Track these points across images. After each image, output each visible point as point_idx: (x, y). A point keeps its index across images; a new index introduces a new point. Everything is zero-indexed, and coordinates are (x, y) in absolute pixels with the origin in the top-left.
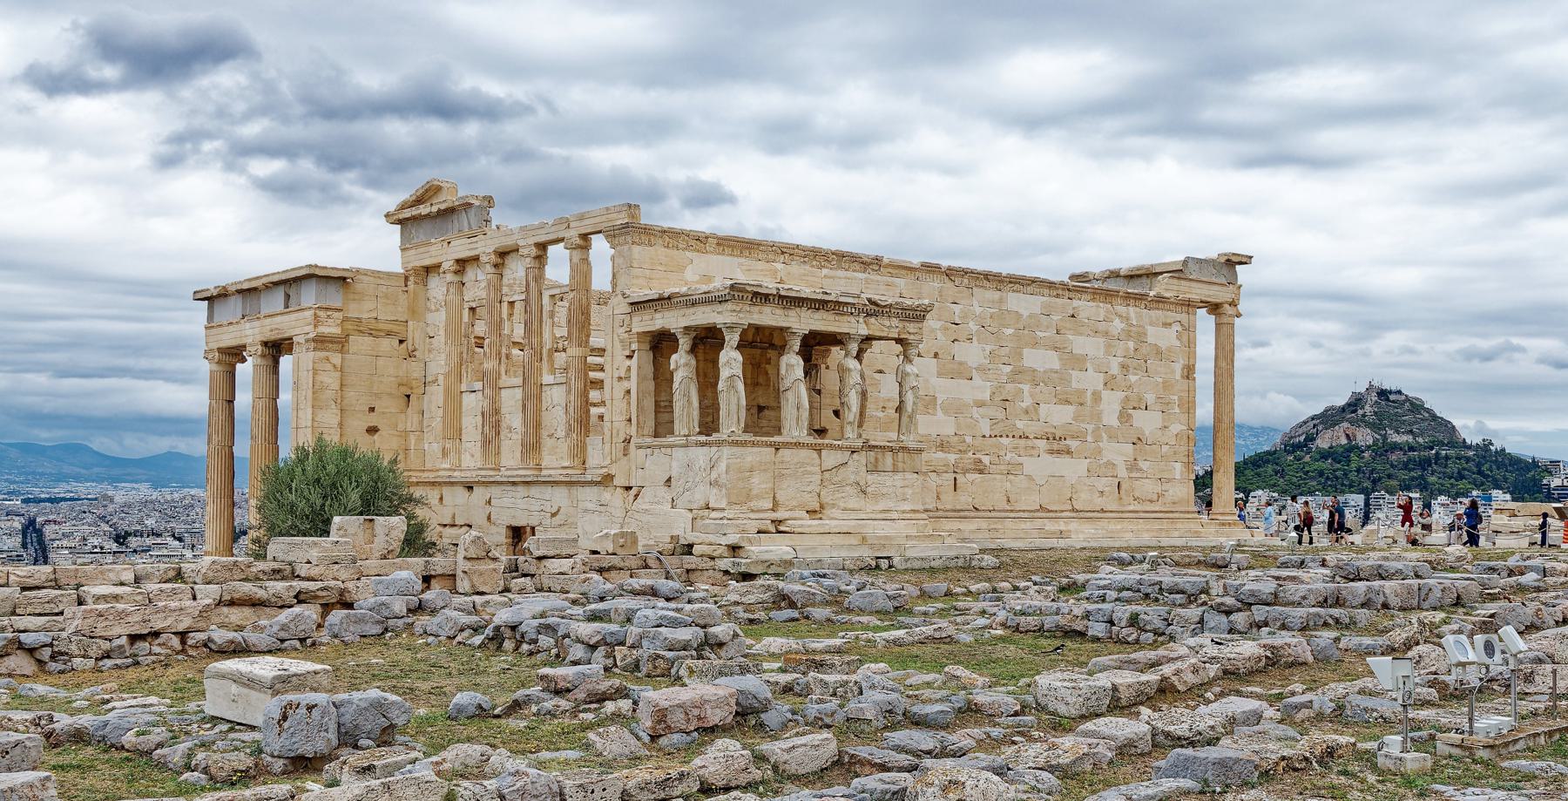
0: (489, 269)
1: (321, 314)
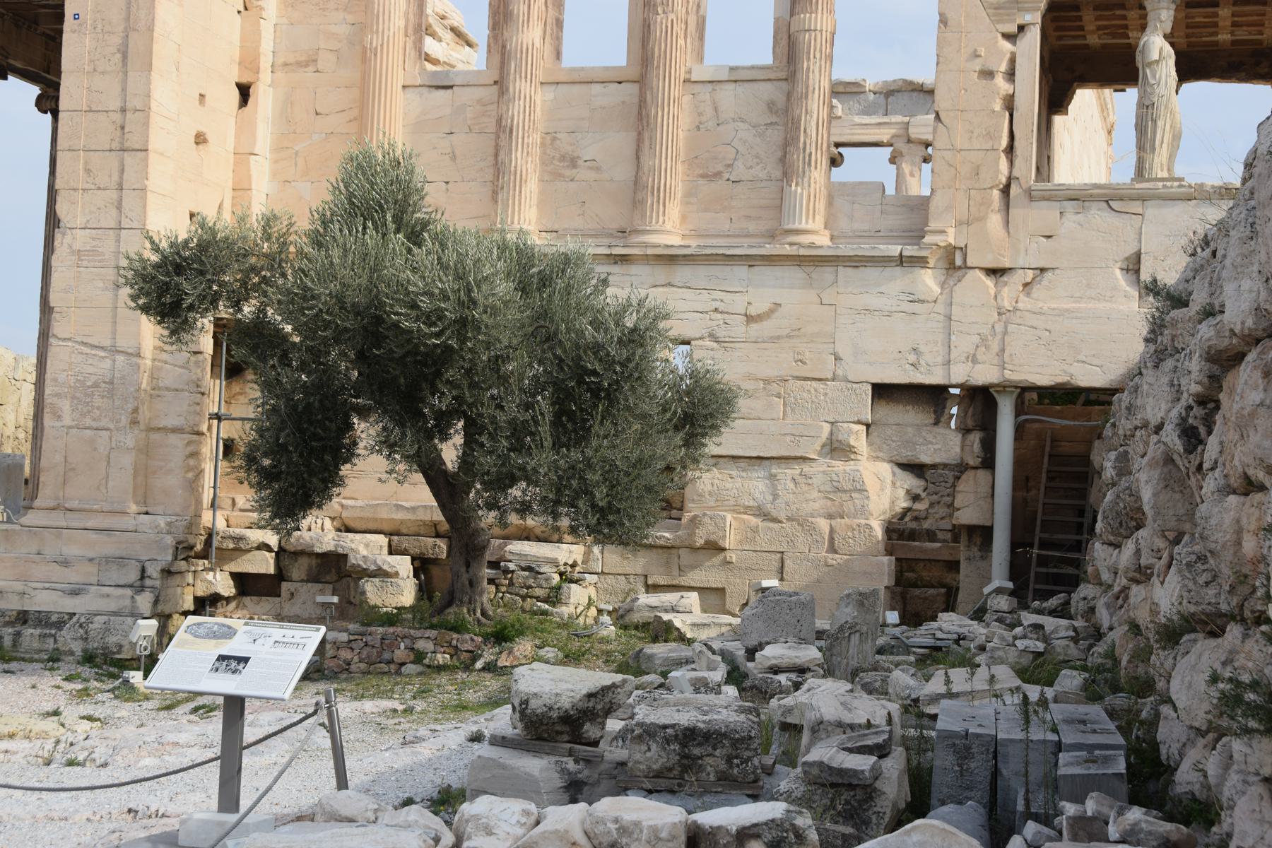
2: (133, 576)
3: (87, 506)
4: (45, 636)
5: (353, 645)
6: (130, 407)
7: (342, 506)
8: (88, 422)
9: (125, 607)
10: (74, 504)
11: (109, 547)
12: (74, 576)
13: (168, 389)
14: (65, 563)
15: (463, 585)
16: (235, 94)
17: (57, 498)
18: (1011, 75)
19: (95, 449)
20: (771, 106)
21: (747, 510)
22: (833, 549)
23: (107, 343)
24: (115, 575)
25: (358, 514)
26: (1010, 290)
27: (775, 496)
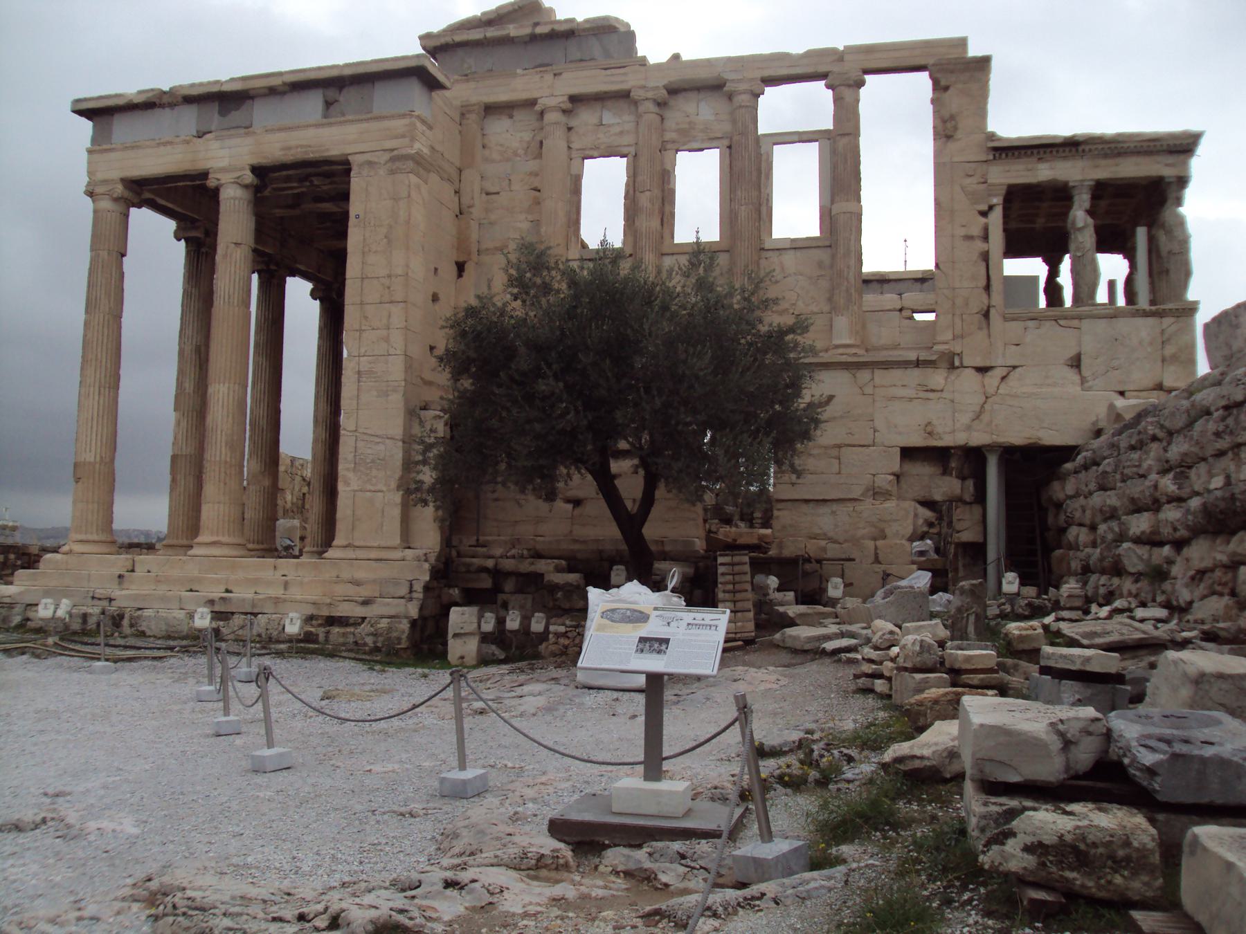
0: (650, 106)
1: (419, 124)
2: (404, 591)
5: (569, 635)
8: (369, 487)
12: (365, 592)
14: (357, 583)
16: (455, 268)
18: (986, 238)
20: (820, 265)
26: (992, 379)
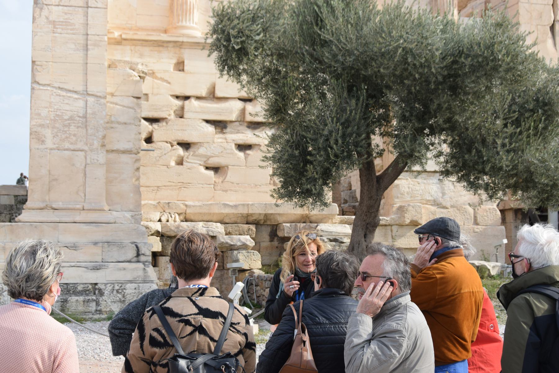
2: (131, 254)
3: (70, 206)
4: (88, 301)
6: (100, 134)
7: (186, 206)
8: (67, 145)
9: (138, 277)
10: (60, 205)
11: (99, 234)
13: (119, 123)
15: (363, 249)
17: (44, 201)
19: (73, 165)
21: (427, 202)
22: (476, 223)
23: (80, 88)
24: (115, 254)
25: (198, 210)
27: (444, 194)
